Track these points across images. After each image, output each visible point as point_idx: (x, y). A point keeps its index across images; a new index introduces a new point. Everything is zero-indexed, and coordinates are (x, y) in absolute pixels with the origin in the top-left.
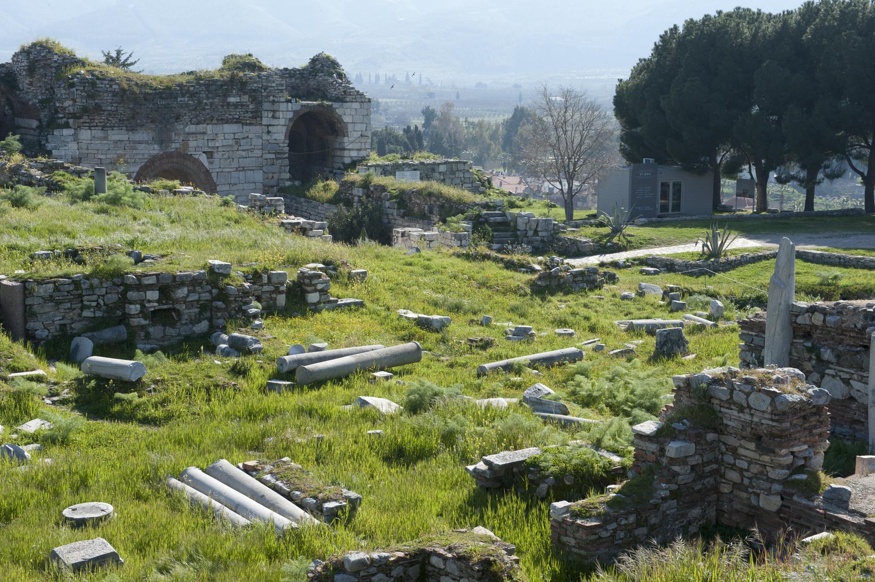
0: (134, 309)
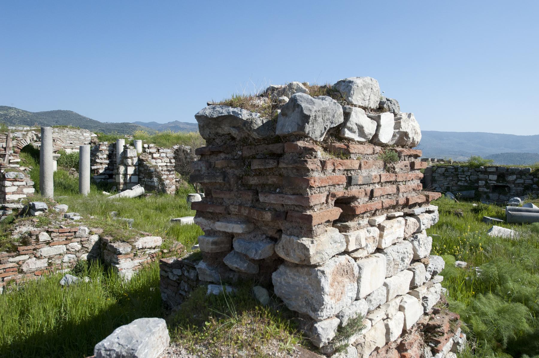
0: (482, 183)
